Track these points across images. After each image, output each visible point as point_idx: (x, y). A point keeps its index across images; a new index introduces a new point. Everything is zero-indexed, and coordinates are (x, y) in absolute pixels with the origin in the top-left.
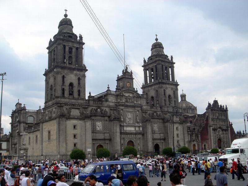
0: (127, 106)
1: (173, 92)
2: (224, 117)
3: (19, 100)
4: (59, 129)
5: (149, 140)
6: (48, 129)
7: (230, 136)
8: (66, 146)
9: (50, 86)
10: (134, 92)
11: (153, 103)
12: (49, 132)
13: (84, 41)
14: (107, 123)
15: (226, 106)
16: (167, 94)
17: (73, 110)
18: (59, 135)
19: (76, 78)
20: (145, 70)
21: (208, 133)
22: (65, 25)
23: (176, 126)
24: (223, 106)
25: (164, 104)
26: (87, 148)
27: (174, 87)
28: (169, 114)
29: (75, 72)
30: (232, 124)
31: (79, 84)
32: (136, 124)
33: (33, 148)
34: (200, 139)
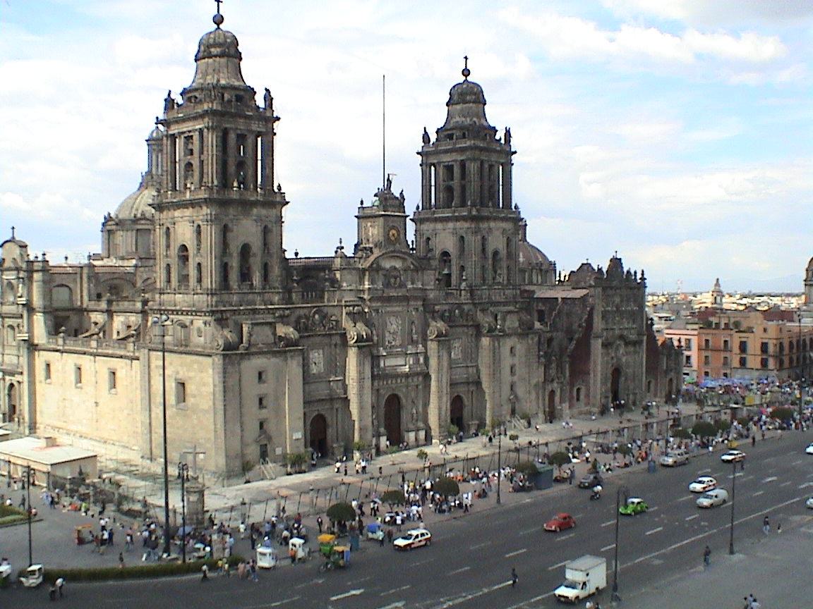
0: (389, 300)
3: (13, 228)
4: (224, 387)
6: (178, 373)
9: (178, 245)
11: (446, 272)
14: (338, 351)
15: (643, 271)
19: (259, 228)
24: (635, 273)
25: (479, 281)
27: (508, 226)
29: (255, 211)
31: (265, 244)
32: (411, 350)
34: (568, 374)
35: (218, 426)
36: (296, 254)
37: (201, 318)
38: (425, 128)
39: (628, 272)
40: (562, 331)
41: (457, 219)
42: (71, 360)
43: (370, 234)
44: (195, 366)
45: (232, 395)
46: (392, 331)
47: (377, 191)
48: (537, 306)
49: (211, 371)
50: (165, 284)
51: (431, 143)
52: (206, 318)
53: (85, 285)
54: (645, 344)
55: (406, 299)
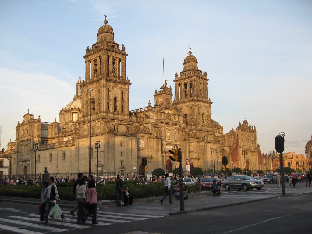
0: (166, 123)
3: (28, 110)
4: (108, 146)
7: (257, 158)
8: (114, 164)
10: (172, 109)
13: (127, 52)
15: (255, 126)
16: (201, 113)
17: (120, 126)
18: (108, 153)
21: (238, 154)
22: (107, 33)
24: (252, 127)
26: (132, 167)
27: (207, 105)
29: (120, 85)
30: (259, 146)
33: (57, 166)
35: (106, 161)
37: (99, 122)
38: (176, 72)
40: (227, 147)
41: (189, 101)
42: (47, 153)
46: (168, 136)
50: (86, 114)
52: (101, 122)
53: (54, 129)
54: (257, 152)
55: (172, 124)
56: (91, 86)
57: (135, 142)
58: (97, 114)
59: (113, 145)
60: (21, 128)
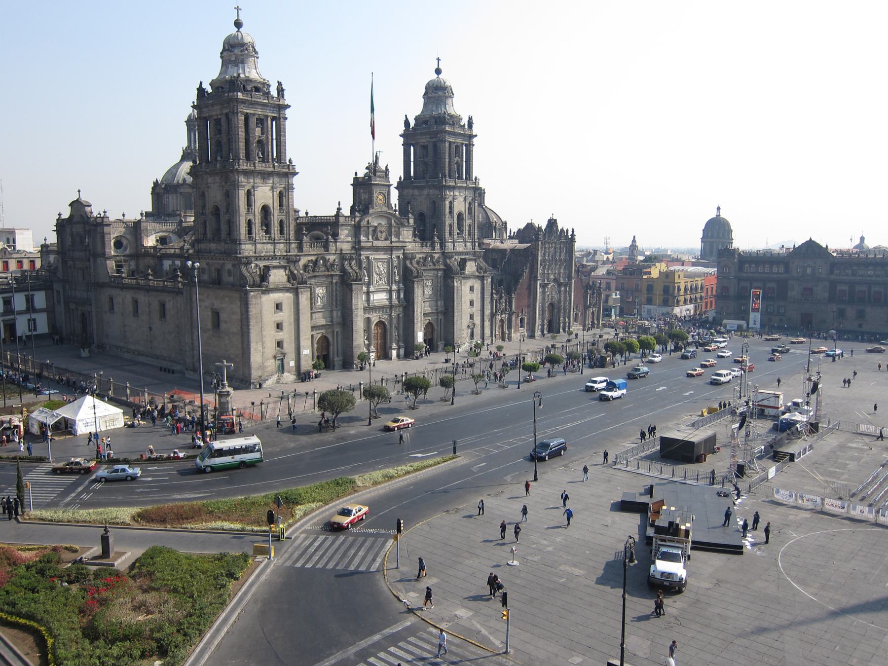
1: (467, 208)
2: (566, 256)
3: (79, 191)
5: (418, 319)
6: (213, 304)
12: (216, 314)
13: (288, 99)
14: (338, 289)
15: (573, 230)
16: (456, 212)
20: (407, 146)
23: (470, 283)
24: (567, 231)
26: (301, 349)
28: (456, 257)
31: (281, 205)
33: (151, 329)
36: (307, 213)
38: (406, 116)
39: (562, 230)
43: (363, 198)
44: (227, 299)
45: (255, 321)
47: (368, 165)
48: (492, 256)
49: (238, 303)
50: (202, 236)
51: (411, 127)
56: (212, 178)
57: (306, 299)
58: (225, 242)
59: (259, 312)
60: (68, 231)
